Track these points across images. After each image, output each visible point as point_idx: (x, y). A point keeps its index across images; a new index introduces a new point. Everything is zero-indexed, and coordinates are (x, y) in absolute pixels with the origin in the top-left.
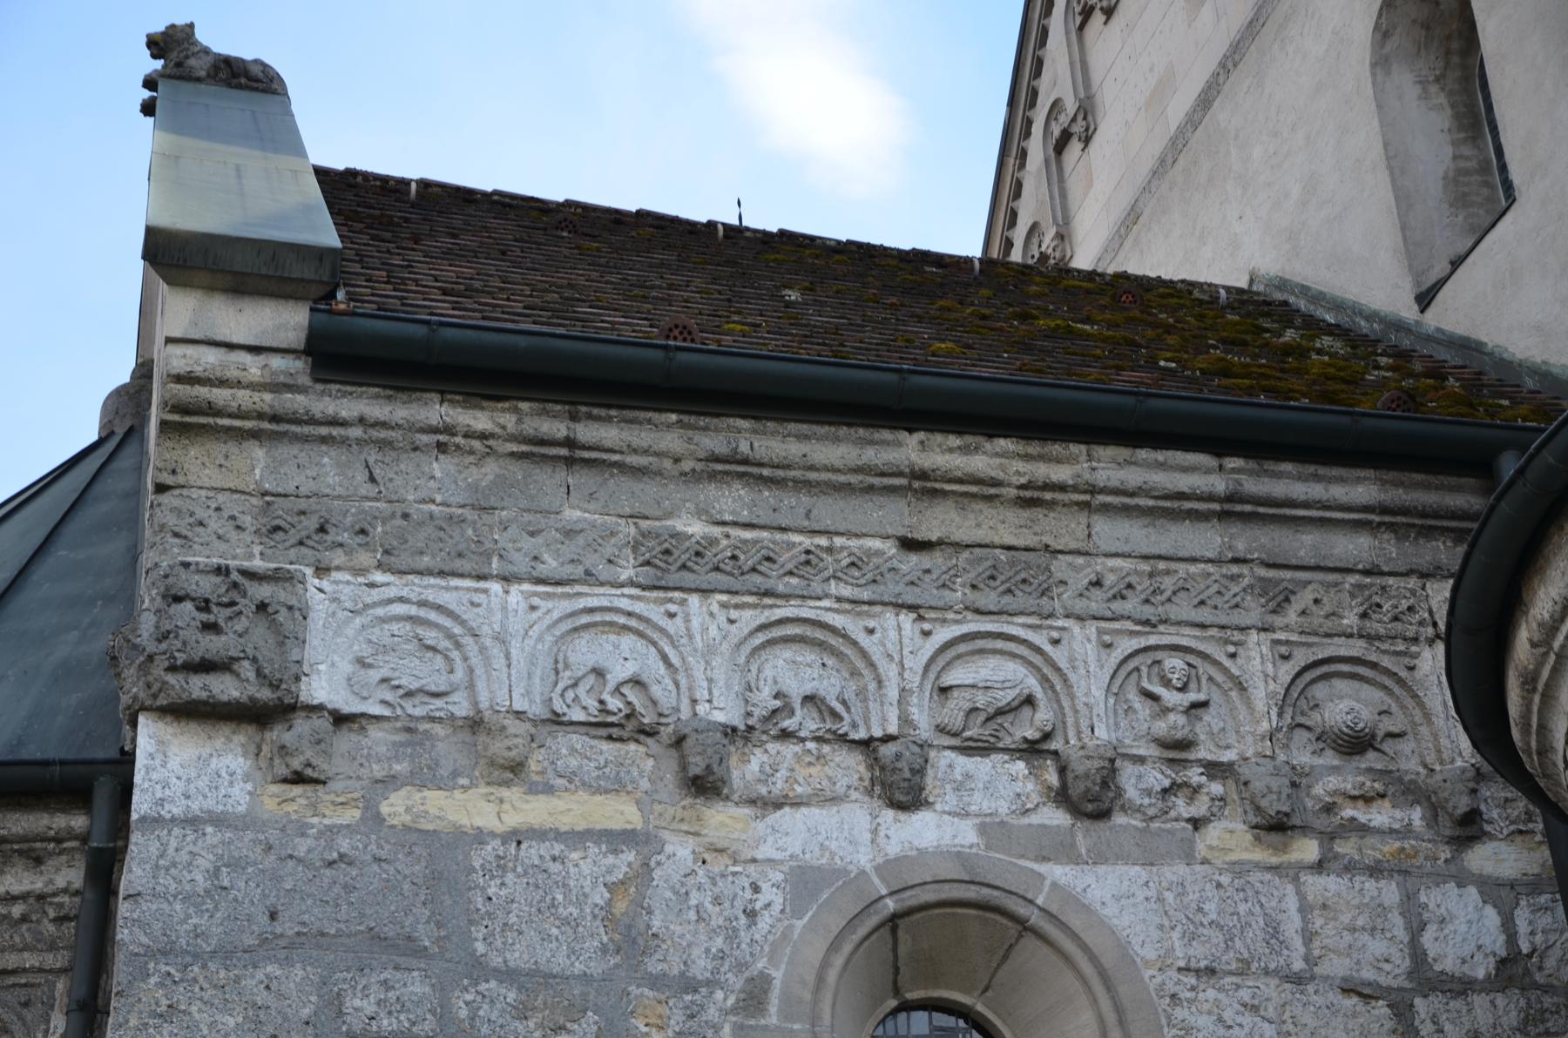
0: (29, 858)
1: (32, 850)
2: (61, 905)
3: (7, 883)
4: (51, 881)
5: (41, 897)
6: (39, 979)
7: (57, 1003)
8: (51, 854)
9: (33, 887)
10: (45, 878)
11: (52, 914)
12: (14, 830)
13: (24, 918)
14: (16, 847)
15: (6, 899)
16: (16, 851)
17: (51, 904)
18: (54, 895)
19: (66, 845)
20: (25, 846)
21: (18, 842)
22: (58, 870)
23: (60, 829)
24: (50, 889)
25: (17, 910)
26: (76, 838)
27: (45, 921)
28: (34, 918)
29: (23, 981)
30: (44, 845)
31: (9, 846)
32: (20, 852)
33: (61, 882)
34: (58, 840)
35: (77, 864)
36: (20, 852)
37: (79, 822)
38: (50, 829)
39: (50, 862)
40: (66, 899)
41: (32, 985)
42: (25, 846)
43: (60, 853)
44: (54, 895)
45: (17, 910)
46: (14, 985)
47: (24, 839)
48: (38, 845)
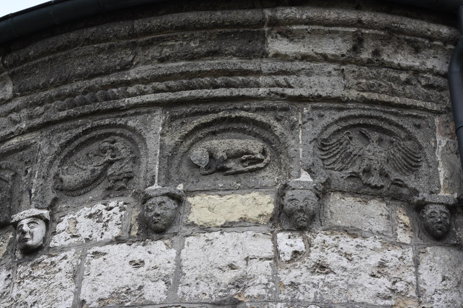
0: (413, 46)
1: (416, 42)
2: (428, 79)
3: (399, 59)
4: (423, 63)
5: (416, 72)
6: (424, 114)
7: (437, 129)
8: (425, 47)
9: (414, 64)
10: (421, 61)
11: (423, 82)
12: (408, 26)
13: (408, 82)
14: (407, 38)
15: (397, 69)
16: (407, 40)
17: (423, 77)
18: (425, 72)
19: (435, 43)
20: (413, 38)
21: (408, 35)
22: (428, 58)
23: (434, 32)
24: (423, 68)
25: (403, 76)
26: (441, 40)
27: (419, 86)
28: (413, 83)
29: (415, 114)
30: (423, 40)
31: (403, 36)
32: (409, 41)
33: (430, 64)
34: (431, 39)
35: (439, 56)
36: (409, 41)
37: (445, 31)
38: (429, 30)
39: (424, 52)
40: (430, 76)
41: (420, 118)
42: (413, 38)
43: (430, 48)
44: (425, 72)
45: (403, 76)
46: (409, 116)
47: (414, 33)
48: (420, 39)
